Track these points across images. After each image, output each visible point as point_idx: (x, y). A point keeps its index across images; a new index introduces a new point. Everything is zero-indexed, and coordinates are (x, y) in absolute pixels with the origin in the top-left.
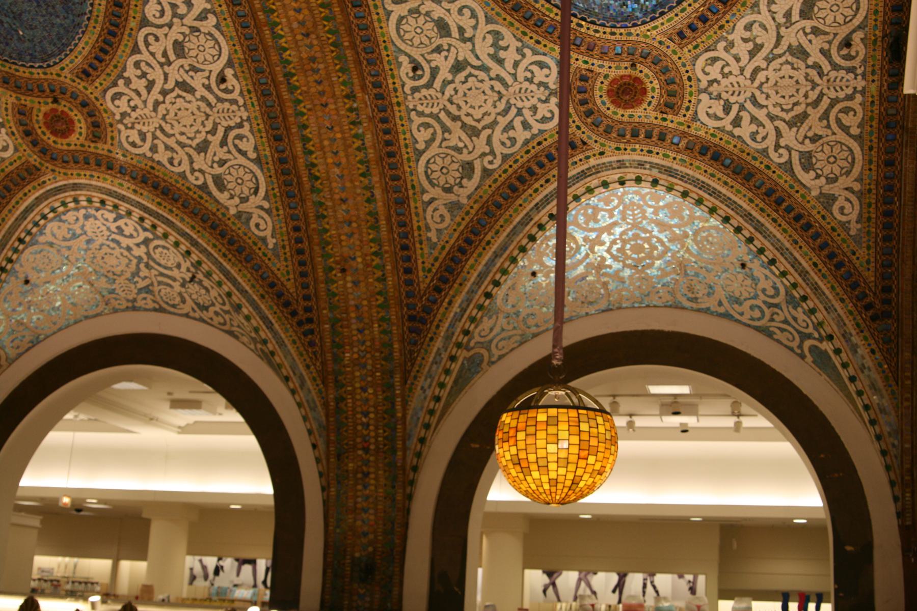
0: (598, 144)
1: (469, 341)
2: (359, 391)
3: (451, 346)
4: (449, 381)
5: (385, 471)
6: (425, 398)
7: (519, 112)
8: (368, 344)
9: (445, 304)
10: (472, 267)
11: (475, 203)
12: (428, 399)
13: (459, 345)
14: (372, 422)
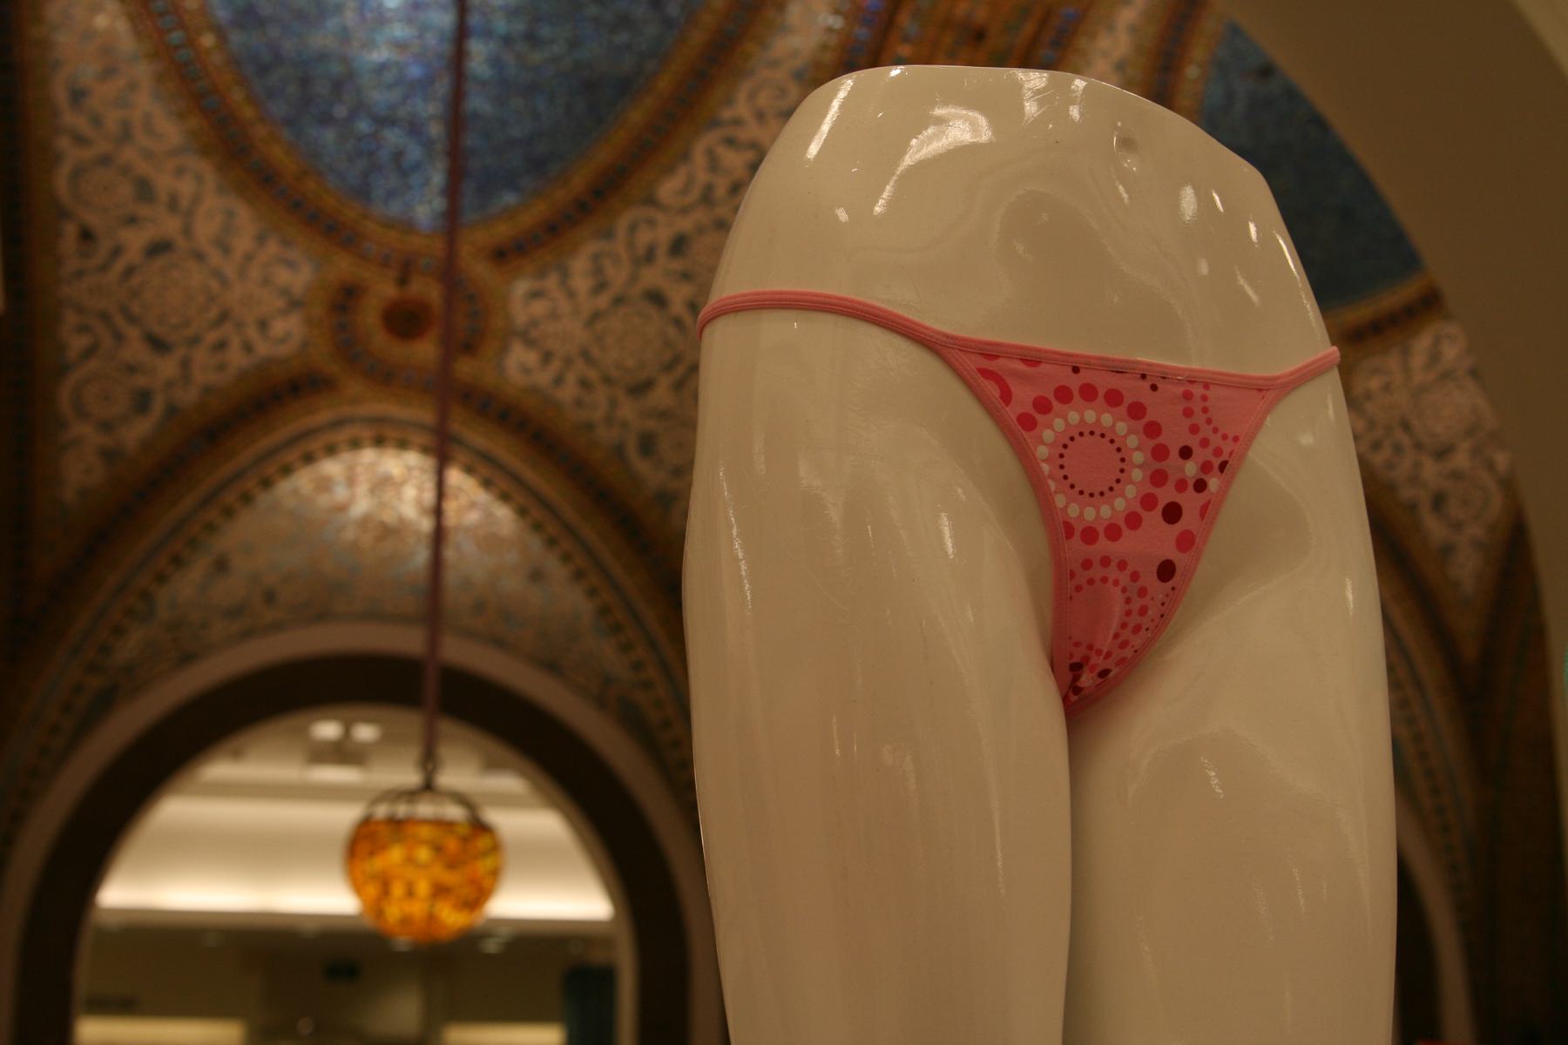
7: (240, 325)
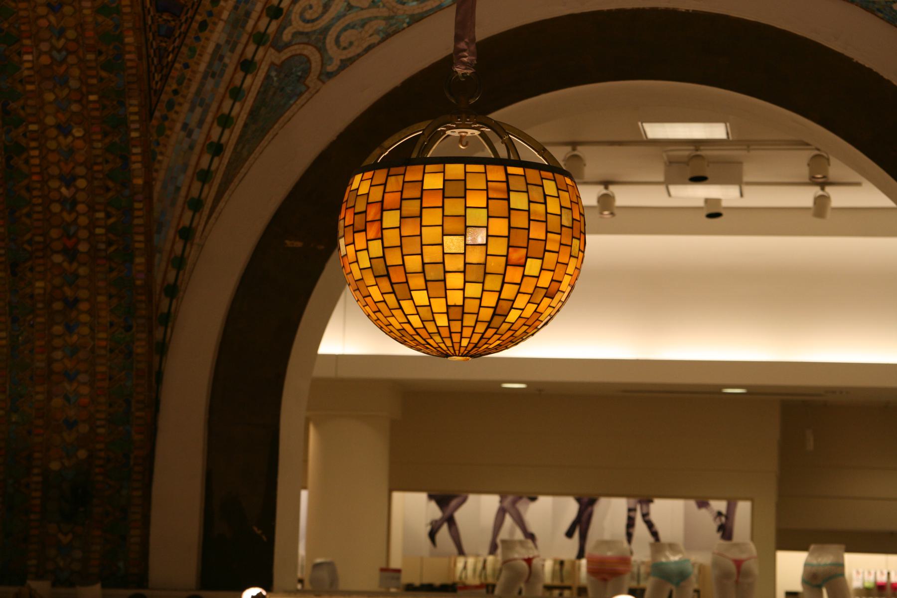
1: (281, 30)
2: (54, 132)
3: (244, 40)
4: (241, 112)
5: (110, 297)
6: (191, 148)
8: (71, 34)
12: (197, 149)
13: (260, 39)
14: (81, 196)
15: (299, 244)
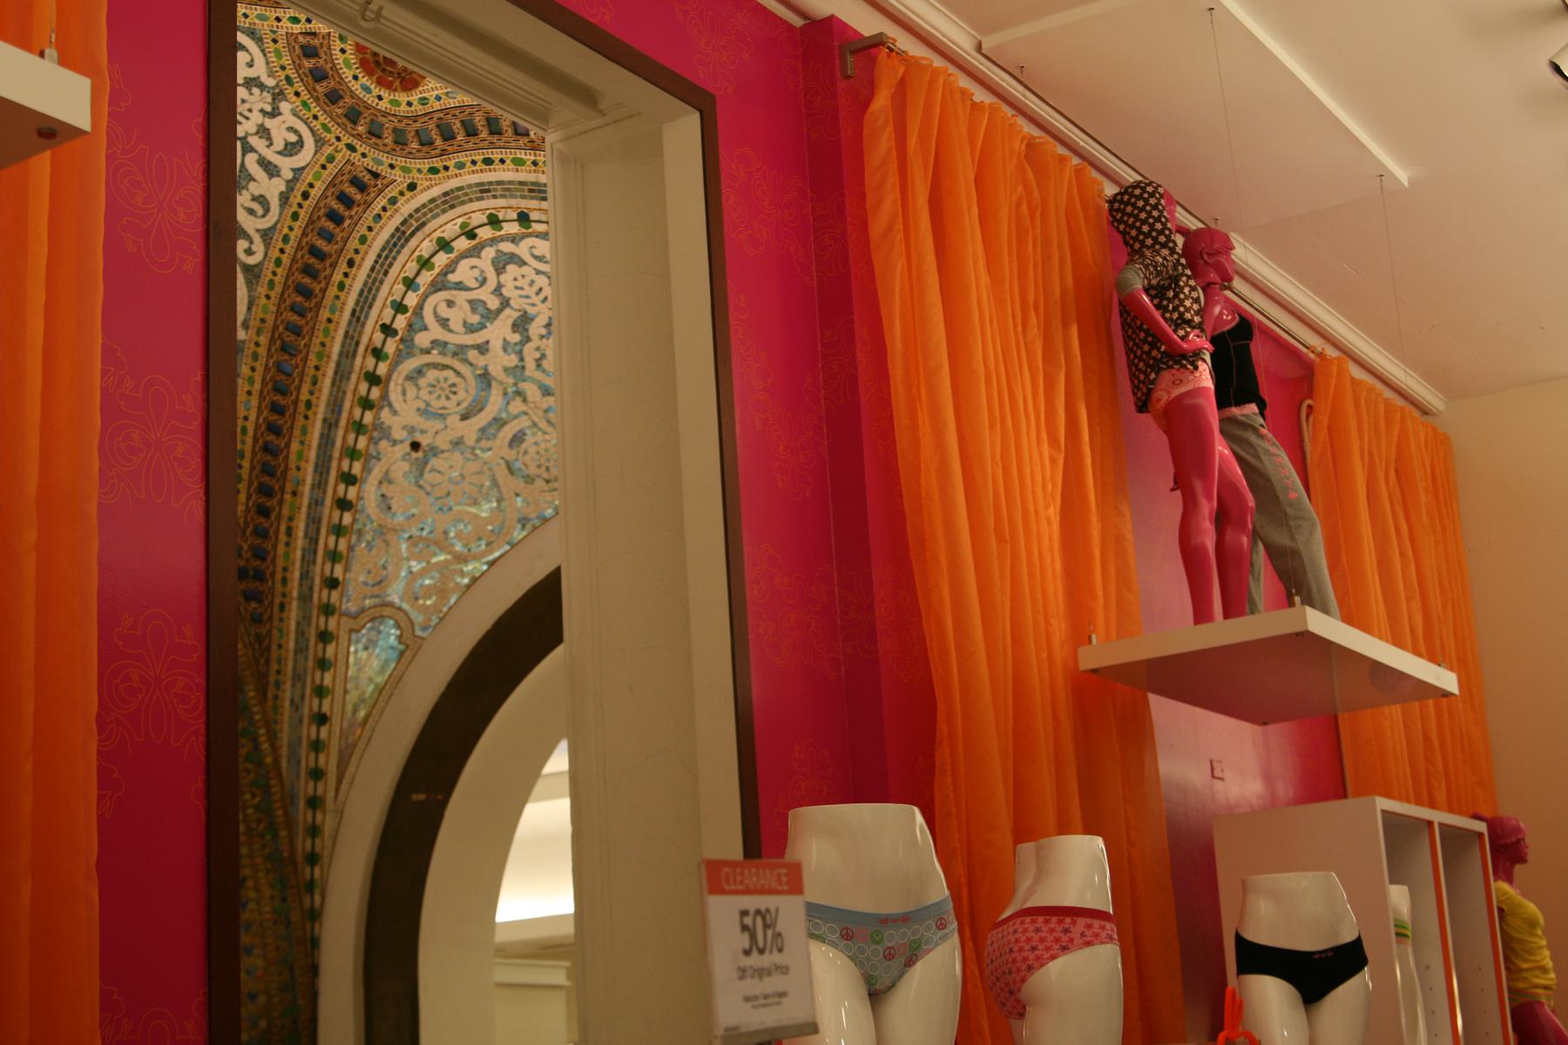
0: (397, 172)
9: (283, 537)
10: (300, 456)
11: (259, 332)
15: (422, 797)
